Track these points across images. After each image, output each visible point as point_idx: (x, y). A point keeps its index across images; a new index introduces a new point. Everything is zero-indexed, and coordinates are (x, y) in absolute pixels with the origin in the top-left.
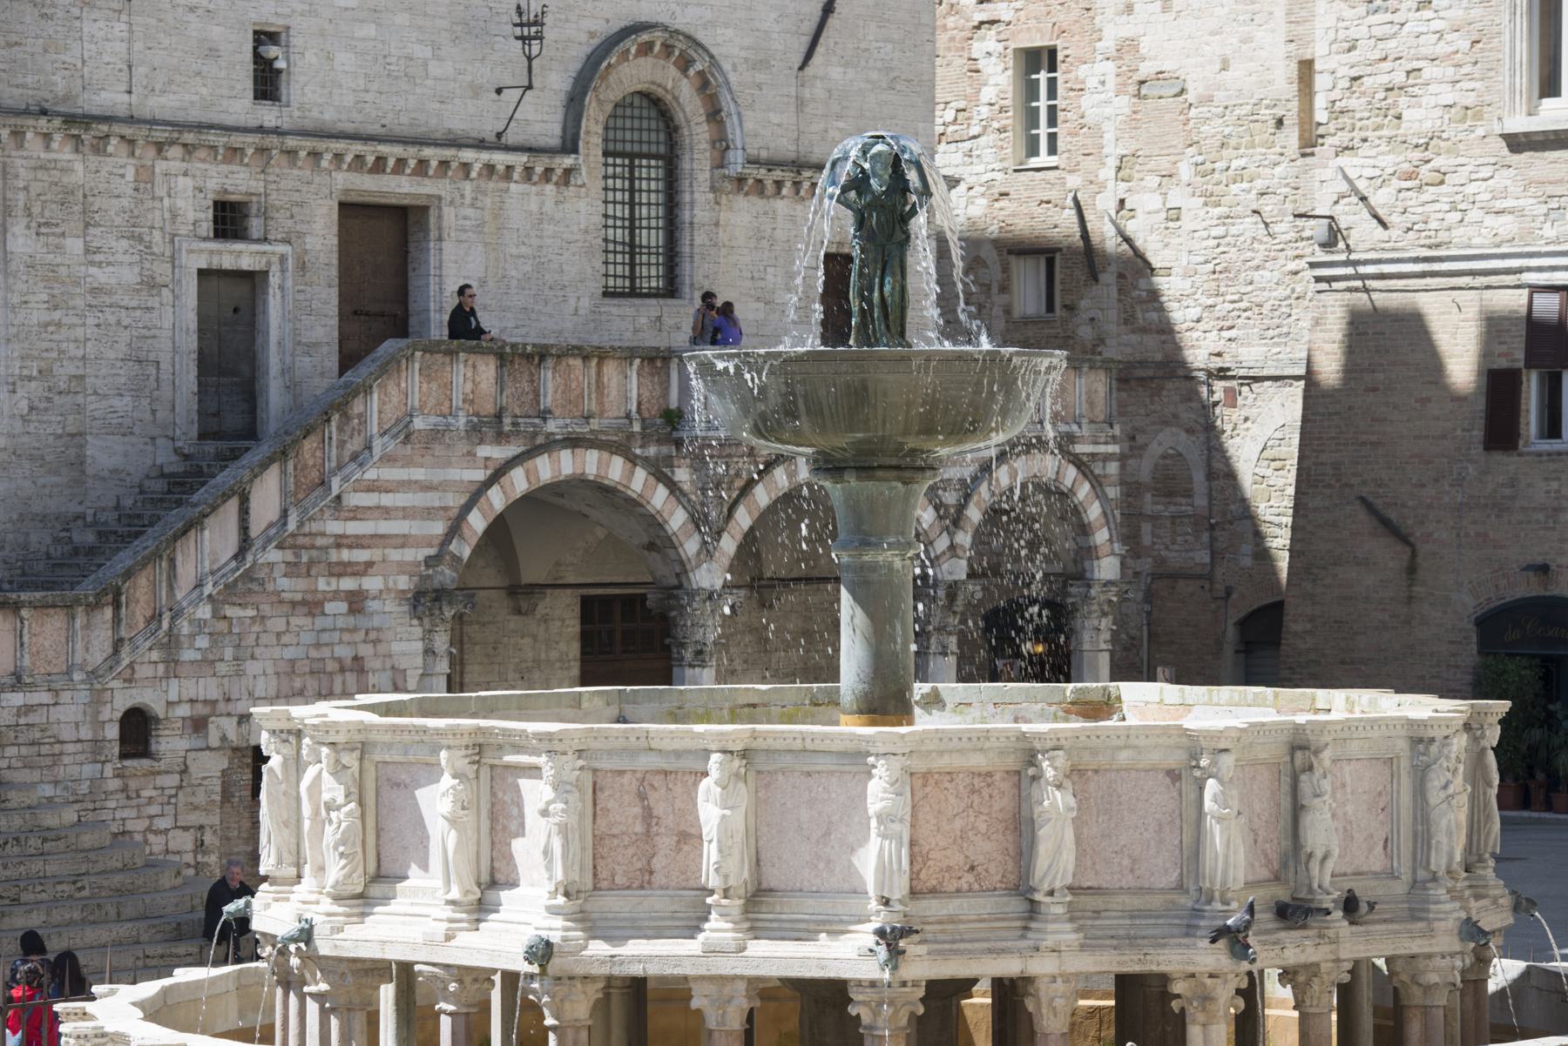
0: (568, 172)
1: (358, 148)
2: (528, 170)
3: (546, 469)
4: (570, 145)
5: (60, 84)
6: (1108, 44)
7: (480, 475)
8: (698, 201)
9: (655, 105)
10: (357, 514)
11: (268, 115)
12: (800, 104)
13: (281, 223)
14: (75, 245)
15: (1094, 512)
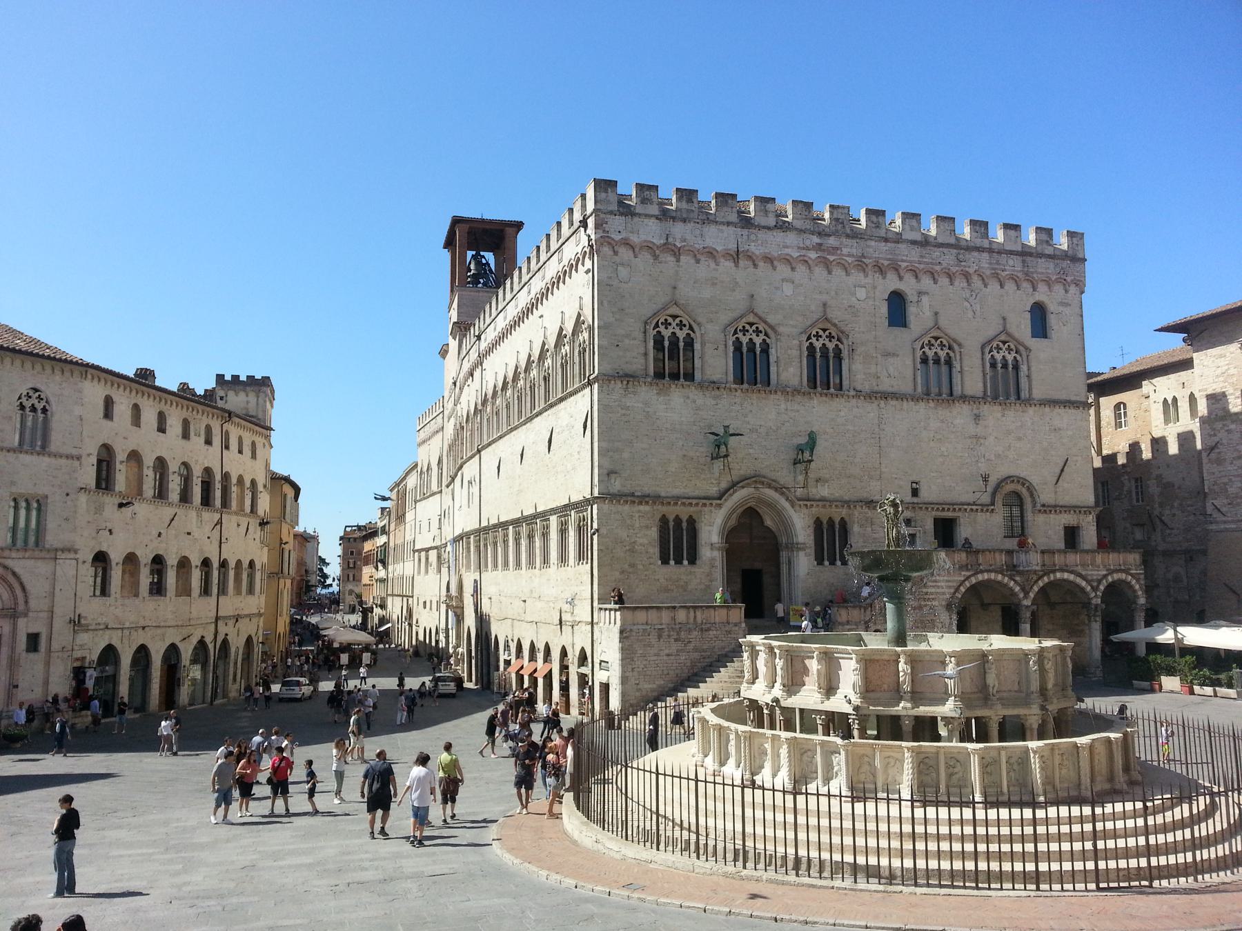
0: (993, 510)
1: (937, 506)
2: (982, 510)
3: (980, 577)
5: (865, 495)
7: (963, 579)
8: (1029, 516)
11: (915, 500)
12: (1056, 492)
15: (1137, 587)
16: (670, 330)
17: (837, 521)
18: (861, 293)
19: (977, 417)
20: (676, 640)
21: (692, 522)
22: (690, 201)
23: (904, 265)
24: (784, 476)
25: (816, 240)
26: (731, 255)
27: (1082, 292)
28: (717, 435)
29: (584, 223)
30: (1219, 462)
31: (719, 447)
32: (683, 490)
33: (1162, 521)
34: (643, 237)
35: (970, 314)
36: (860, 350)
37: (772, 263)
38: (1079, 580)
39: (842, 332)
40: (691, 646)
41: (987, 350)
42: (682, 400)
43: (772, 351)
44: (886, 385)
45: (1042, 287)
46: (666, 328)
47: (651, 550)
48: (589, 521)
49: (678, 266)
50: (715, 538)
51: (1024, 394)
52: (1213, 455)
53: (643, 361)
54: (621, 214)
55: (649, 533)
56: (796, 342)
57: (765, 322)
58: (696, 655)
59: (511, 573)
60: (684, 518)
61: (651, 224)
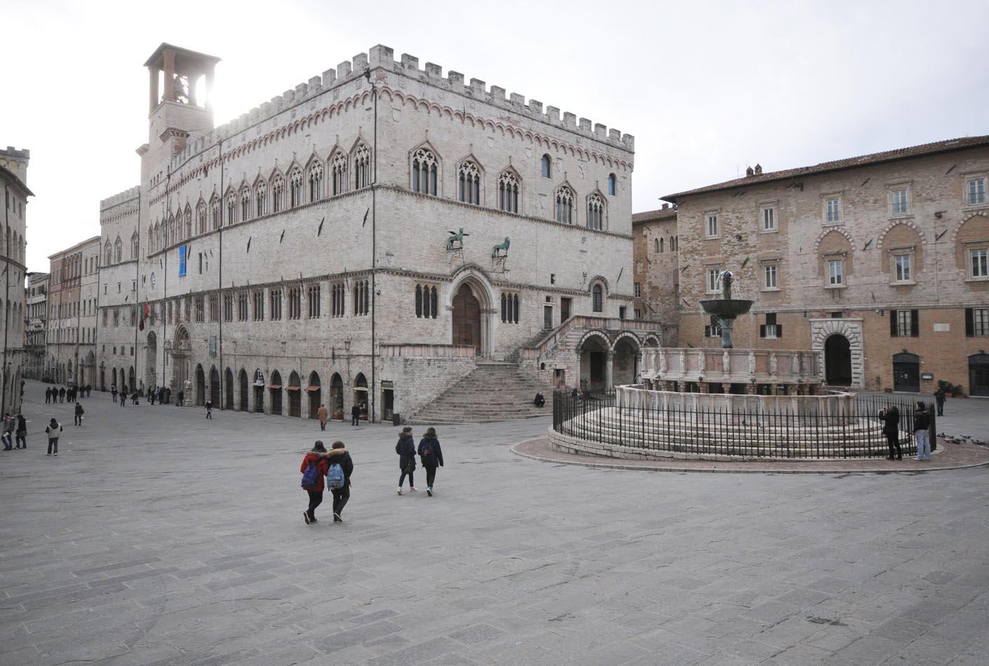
3: (592, 333)
4: (589, 291)
6: (647, 281)
7: (583, 334)
8: (604, 299)
9: (598, 286)
10: (569, 338)
13: (554, 300)
17: (513, 294)
18: (529, 153)
19: (584, 239)
20: (439, 367)
21: (434, 289)
24: (485, 263)
26: (459, 114)
27: (632, 171)
30: (688, 276)
31: (452, 241)
33: (650, 308)
38: (634, 337)
39: (519, 176)
40: (446, 372)
41: (589, 199)
43: (481, 182)
44: (539, 215)
45: (615, 165)
50: (449, 303)
55: (410, 295)
56: (494, 178)
57: (478, 163)
58: (449, 377)
59: (250, 323)
60: (430, 287)
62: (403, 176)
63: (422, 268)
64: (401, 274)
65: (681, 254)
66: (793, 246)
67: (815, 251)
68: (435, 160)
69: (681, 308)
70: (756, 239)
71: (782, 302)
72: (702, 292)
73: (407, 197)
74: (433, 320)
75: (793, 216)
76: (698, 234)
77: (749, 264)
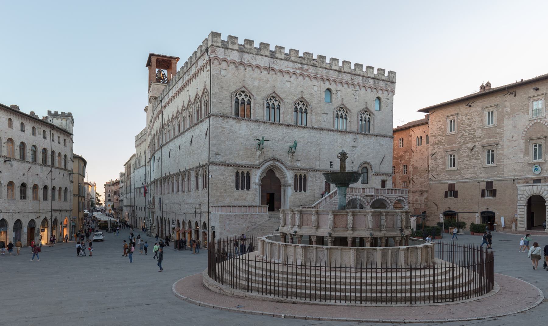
6: (411, 164)
12: (380, 168)
14: (314, 179)
16: (242, 97)
17: (303, 175)
18: (316, 88)
19: (355, 140)
21: (248, 174)
22: (251, 45)
23: (332, 79)
24: (285, 157)
25: (299, 65)
28: (259, 140)
29: (207, 50)
30: (435, 159)
31: (259, 145)
32: (245, 161)
33: (413, 180)
34: (232, 58)
35: (354, 100)
36: (314, 110)
37: (282, 73)
39: (308, 103)
42: (246, 126)
43: (281, 109)
44: (323, 125)
46: (240, 96)
47: (232, 185)
48: (208, 172)
49: (245, 71)
51: (371, 132)
52: (433, 157)
53: (230, 109)
54: (223, 48)
55: (232, 177)
56: (290, 106)
57: (279, 97)
60: (245, 172)
61: (234, 53)
62: (228, 108)
63: (240, 161)
64: (225, 165)
65: (431, 145)
66: (507, 135)
67: (523, 138)
68: (250, 97)
69: (430, 180)
70: (481, 132)
71: (498, 174)
72: (444, 169)
73: (230, 121)
74: (247, 191)
75: (507, 115)
76: (442, 132)
77: (475, 149)
